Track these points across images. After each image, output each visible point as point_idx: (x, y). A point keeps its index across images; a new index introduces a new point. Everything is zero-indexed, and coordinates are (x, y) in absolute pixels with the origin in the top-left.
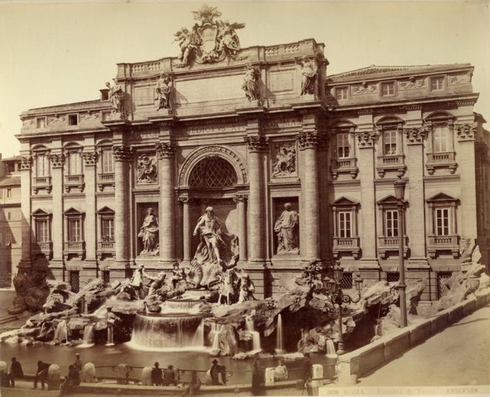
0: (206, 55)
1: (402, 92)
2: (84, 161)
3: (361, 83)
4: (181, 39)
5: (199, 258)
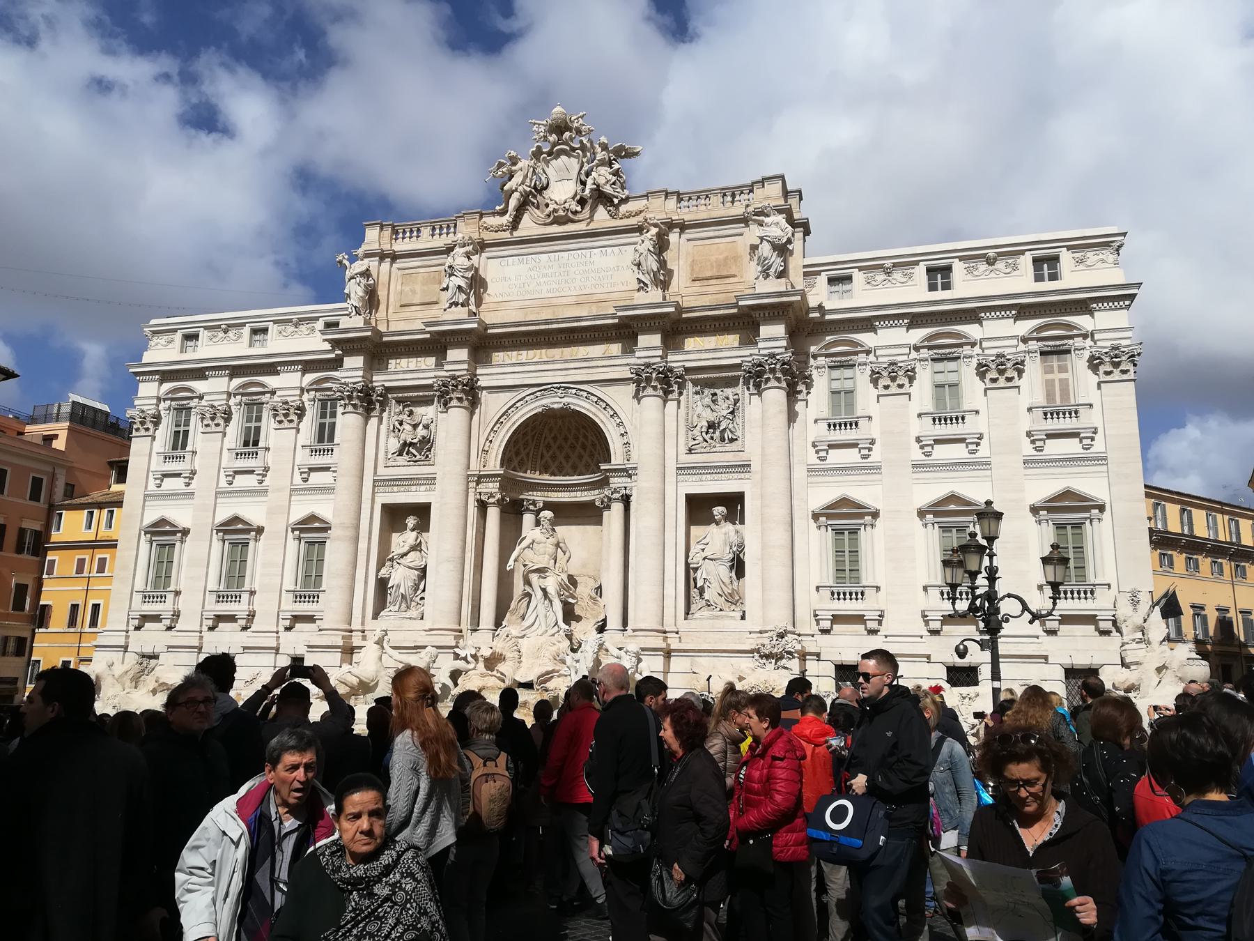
0: (556, 207)
1: (967, 285)
5: (511, 626)
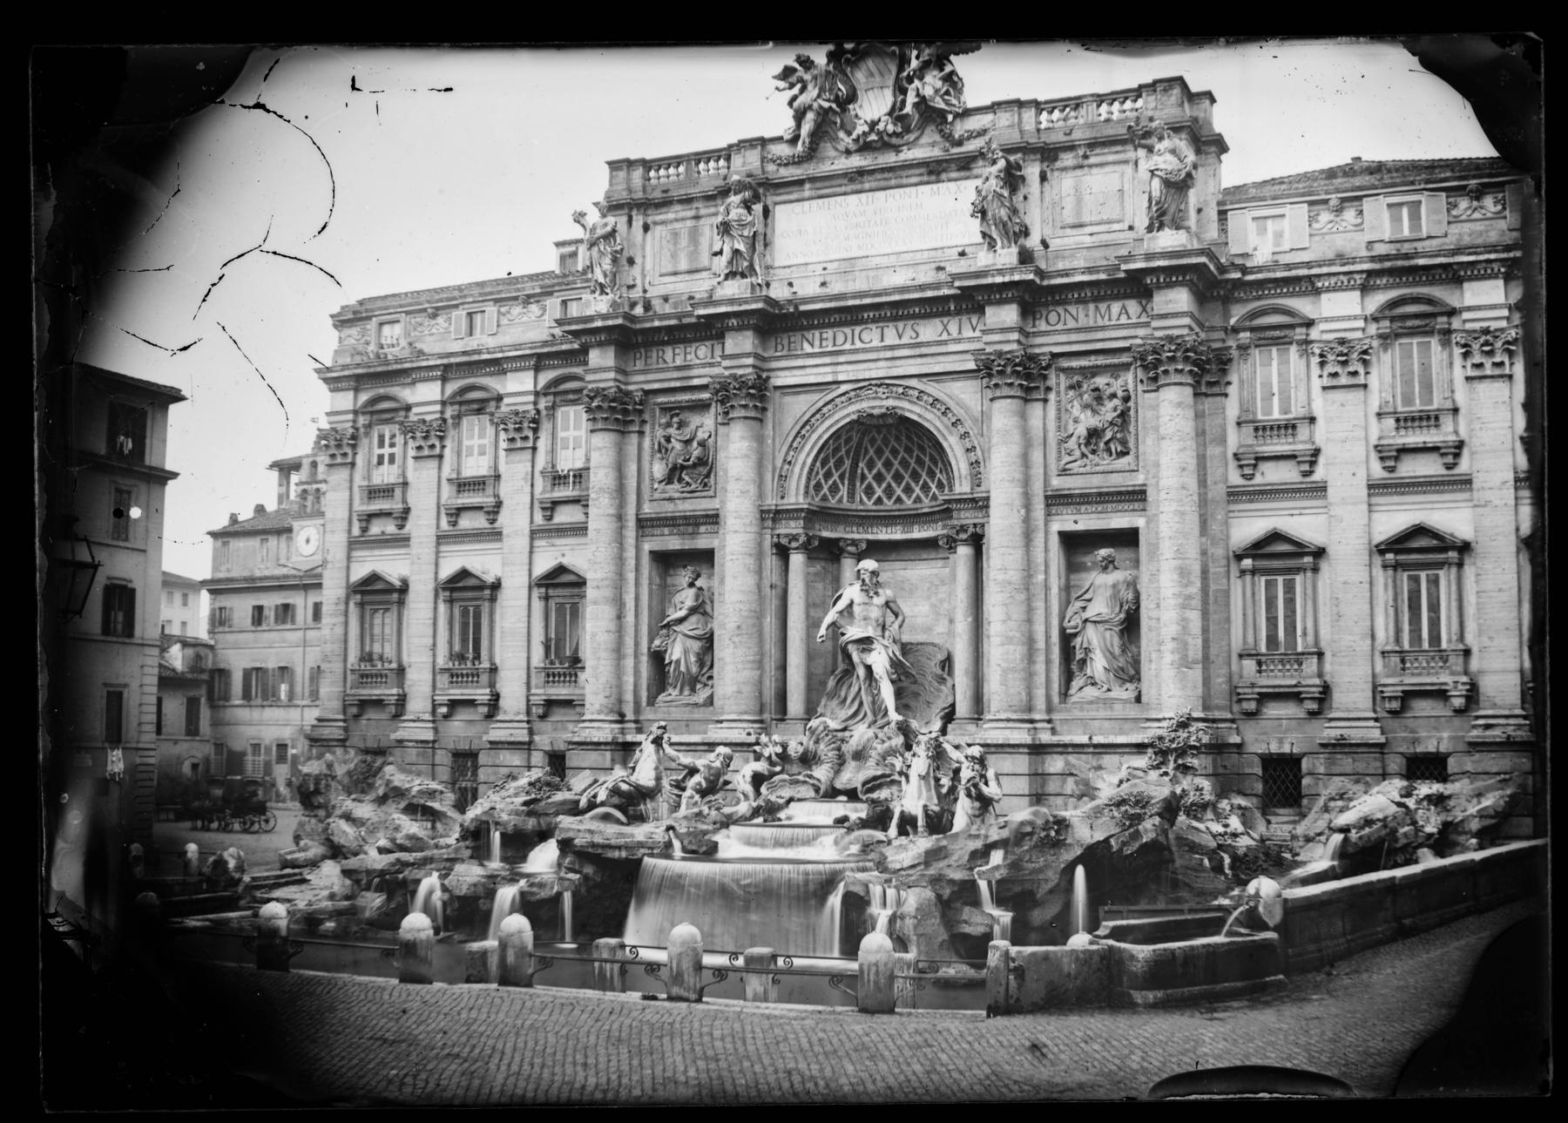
2: (503, 436)
3: (1326, 202)
4: (792, 86)
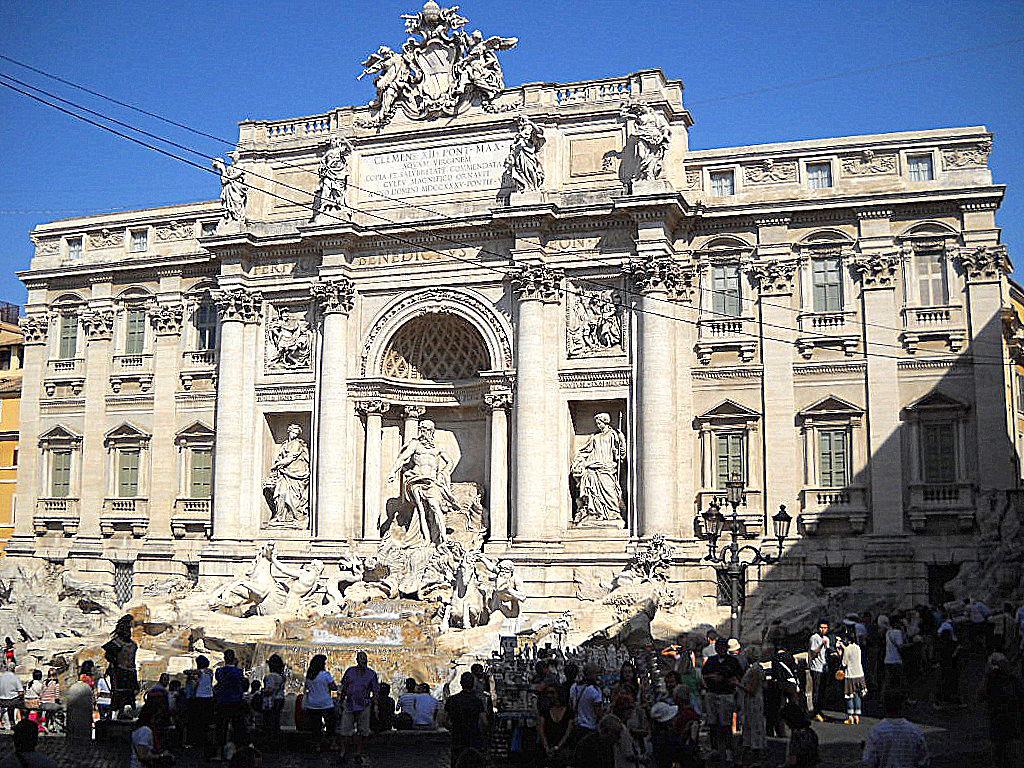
0: (431, 102)
